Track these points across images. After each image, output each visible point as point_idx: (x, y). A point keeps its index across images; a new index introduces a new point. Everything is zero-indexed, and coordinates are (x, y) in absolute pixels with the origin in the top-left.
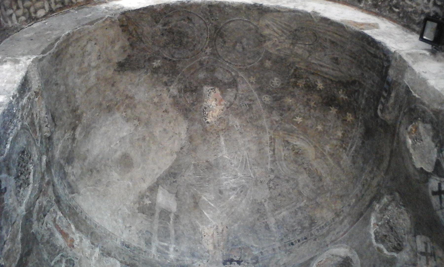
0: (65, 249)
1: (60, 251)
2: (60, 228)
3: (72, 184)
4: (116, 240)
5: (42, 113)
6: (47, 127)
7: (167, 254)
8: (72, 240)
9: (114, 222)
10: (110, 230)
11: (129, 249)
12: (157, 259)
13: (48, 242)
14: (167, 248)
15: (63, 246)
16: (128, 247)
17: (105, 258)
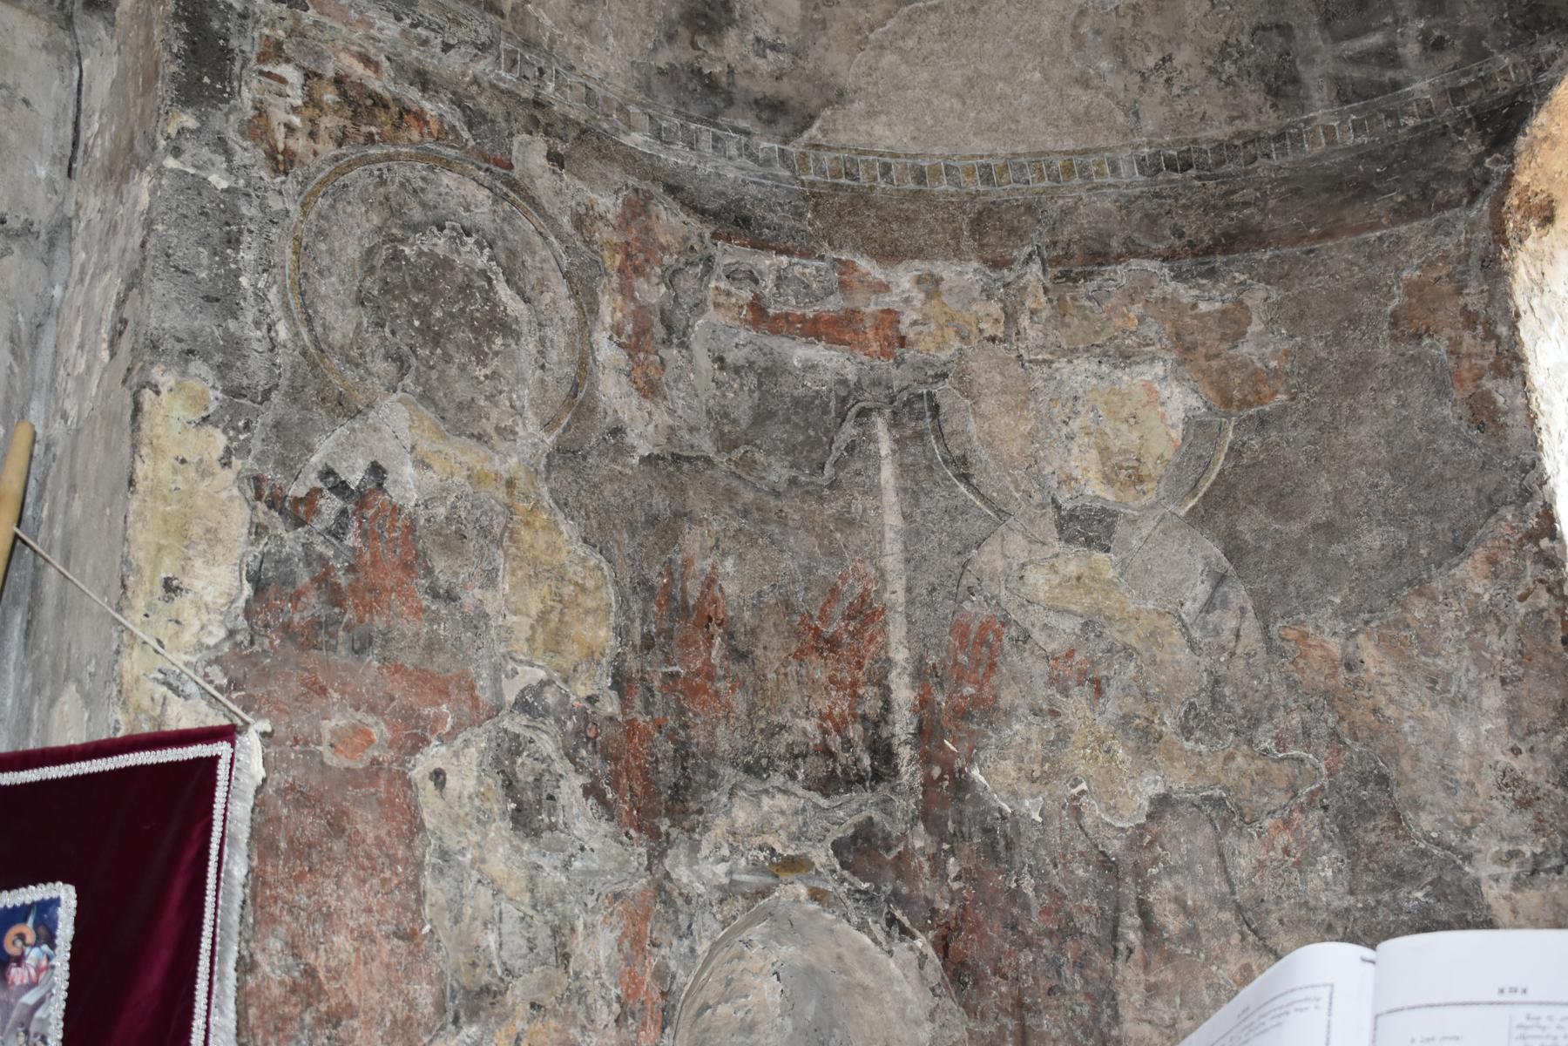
0: (865, 382)
1: (844, 400)
2: (802, 319)
3: (786, 89)
4: (1115, 169)
5: (381, 29)
6: (452, 52)
7: (1396, 85)
8: (890, 317)
9: (1076, 91)
10: (1069, 144)
11: (1192, 172)
12: (1350, 140)
13: (762, 417)
14: (1388, 57)
15: (851, 372)
16: (1187, 166)
17: (1087, 287)
